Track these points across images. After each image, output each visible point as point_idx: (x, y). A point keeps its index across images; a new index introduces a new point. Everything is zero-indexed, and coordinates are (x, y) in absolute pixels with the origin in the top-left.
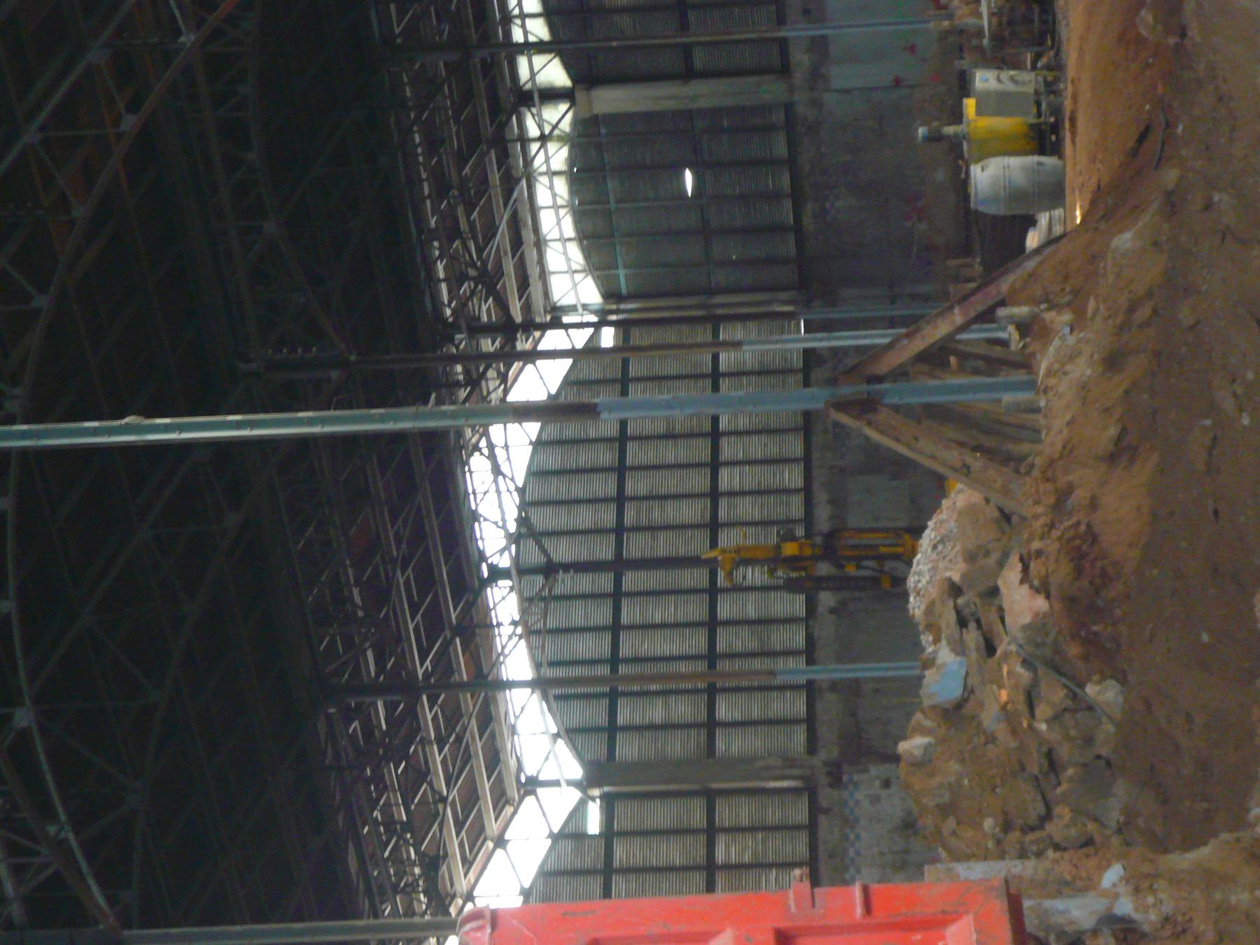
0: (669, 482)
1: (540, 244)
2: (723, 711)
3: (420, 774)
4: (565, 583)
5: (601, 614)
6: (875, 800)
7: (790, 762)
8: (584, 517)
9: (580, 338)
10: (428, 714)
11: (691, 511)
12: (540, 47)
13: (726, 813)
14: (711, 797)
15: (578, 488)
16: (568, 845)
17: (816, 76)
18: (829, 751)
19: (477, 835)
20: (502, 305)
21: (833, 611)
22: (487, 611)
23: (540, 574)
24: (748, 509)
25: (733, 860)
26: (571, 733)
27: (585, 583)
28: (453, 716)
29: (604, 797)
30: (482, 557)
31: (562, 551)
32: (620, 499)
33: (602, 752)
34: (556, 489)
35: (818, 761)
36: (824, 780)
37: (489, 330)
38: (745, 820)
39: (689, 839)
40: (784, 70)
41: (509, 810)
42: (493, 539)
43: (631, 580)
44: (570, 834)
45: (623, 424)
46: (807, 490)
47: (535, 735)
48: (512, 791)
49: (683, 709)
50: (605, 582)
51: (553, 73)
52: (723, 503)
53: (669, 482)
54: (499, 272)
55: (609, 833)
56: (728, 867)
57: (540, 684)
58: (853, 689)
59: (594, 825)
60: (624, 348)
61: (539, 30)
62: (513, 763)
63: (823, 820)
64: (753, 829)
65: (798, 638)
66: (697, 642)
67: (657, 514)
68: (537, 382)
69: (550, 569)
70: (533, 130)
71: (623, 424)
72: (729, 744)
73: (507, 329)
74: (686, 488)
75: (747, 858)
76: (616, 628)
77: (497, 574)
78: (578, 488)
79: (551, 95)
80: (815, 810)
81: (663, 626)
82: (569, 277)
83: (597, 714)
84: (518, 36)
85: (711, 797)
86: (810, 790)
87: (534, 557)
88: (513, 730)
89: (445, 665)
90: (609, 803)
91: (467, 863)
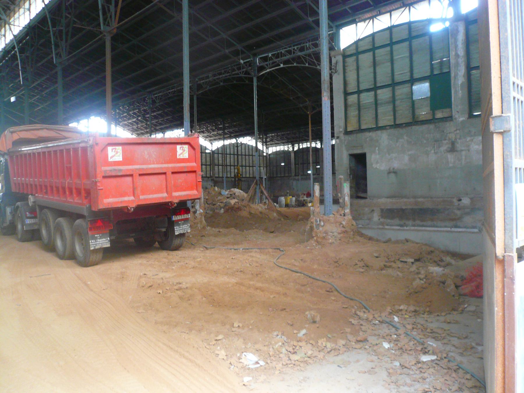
0: (247, 161)
1: (276, 146)
2: (220, 167)
3: (213, 131)
4: (236, 148)
7: (214, 175)
8: (243, 151)
9: (265, 151)
10: (220, 132)
11: (244, 164)
12: (299, 147)
13: (208, 167)
14: (210, 165)
15: (247, 150)
17: (295, 179)
19: (206, 137)
20: (269, 142)
23: (237, 145)
24: (244, 170)
26: (218, 149)
27: (236, 151)
28: (220, 135)
31: (239, 148)
34: (247, 148)
37: (266, 140)
40: (295, 176)
43: (236, 156)
44: (206, 148)
46: (246, 177)
47: (218, 144)
49: (220, 162)
50: (236, 153)
51: (296, 148)
53: (247, 161)
55: (206, 153)
59: (207, 151)
60: (264, 156)
61: (301, 147)
65: (229, 176)
68: (260, 146)
69: (237, 147)
70: (289, 146)
72: (216, 168)
73: (266, 142)
77: (237, 140)
78: (247, 150)
79: (293, 148)
80: (208, 177)
82: (272, 150)
85: (210, 165)
86: (211, 177)
89: (227, 134)
90: (210, 153)
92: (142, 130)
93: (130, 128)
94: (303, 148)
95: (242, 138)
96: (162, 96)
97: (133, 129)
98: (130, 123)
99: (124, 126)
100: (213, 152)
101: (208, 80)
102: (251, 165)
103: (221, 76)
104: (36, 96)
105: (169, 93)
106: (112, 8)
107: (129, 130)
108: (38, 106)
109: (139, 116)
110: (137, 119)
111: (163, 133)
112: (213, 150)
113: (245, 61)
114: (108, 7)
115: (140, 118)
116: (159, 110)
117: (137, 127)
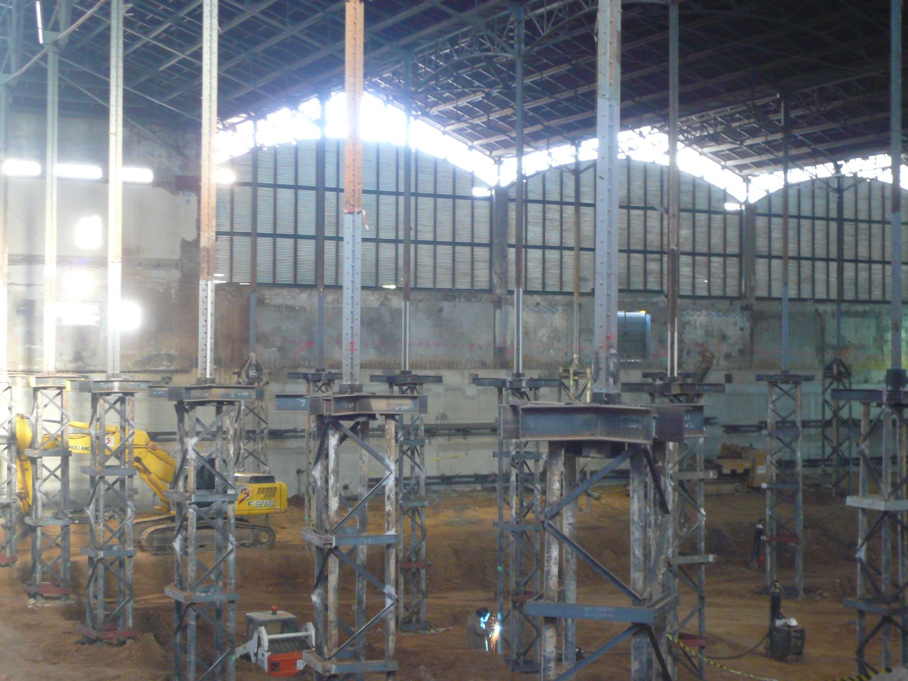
0: (877, 244)
2: (776, 263)
3: (753, 133)
4: (834, 197)
5: (863, 216)
6: (735, 324)
7: (753, 289)
8: (863, 206)
10: (779, 136)
11: (863, 252)
14: (739, 256)
15: (876, 203)
16: (721, 196)
18: (758, 306)
19: (727, 158)
21: (817, 310)
22: (823, 163)
24: (863, 275)
25: (712, 264)
26: (769, 198)
27: (833, 206)
29: (741, 210)
30: (846, 161)
31: (848, 196)
32: (870, 221)
33: (760, 211)
34: (877, 195)
35: (752, 301)
36: (744, 303)
38: (728, 270)
39: (721, 246)
41: (737, 171)
43: (833, 226)
44: (725, 197)
45: (889, 223)
46: (870, 302)
47: (767, 183)
48: (745, 172)
49: (777, 246)
50: (833, 214)
52: (866, 266)
53: (877, 244)
55: (725, 213)
56: (709, 262)
57: (787, 186)
58: (779, 317)
59: (730, 207)
62: (757, 173)
63: (727, 302)
64: (725, 272)
65: (806, 294)
66: (806, 252)
67: (863, 237)
69: (840, 191)
71: (889, 223)
72: (761, 265)
74: (873, 250)
75: (713, 270)
76: (813, 218)
77: (838, 168)
78: (876, 203)
80: (732, 299)
81: (813, 238)
83: (777, 209)
85: (739, 256)
86: (741, 297)
87: (846, 184)
88: (771, 173)
89: (798, 144)
90: (739, 213)
91: (715, 154)
92: (503, 132)
95: (859, 160)
96: (560, 11)
97: (474, 127)
98: (463, 109)
99: (444, 119)
100: (750, 213)
104: (160, 23)
107: (460, 131)
108: (170, 55)
109: (492, 85)
110: (488, 96)
111: (573, 143)
112: (752, 201)
115: (495, 93)
116: (558, 63)
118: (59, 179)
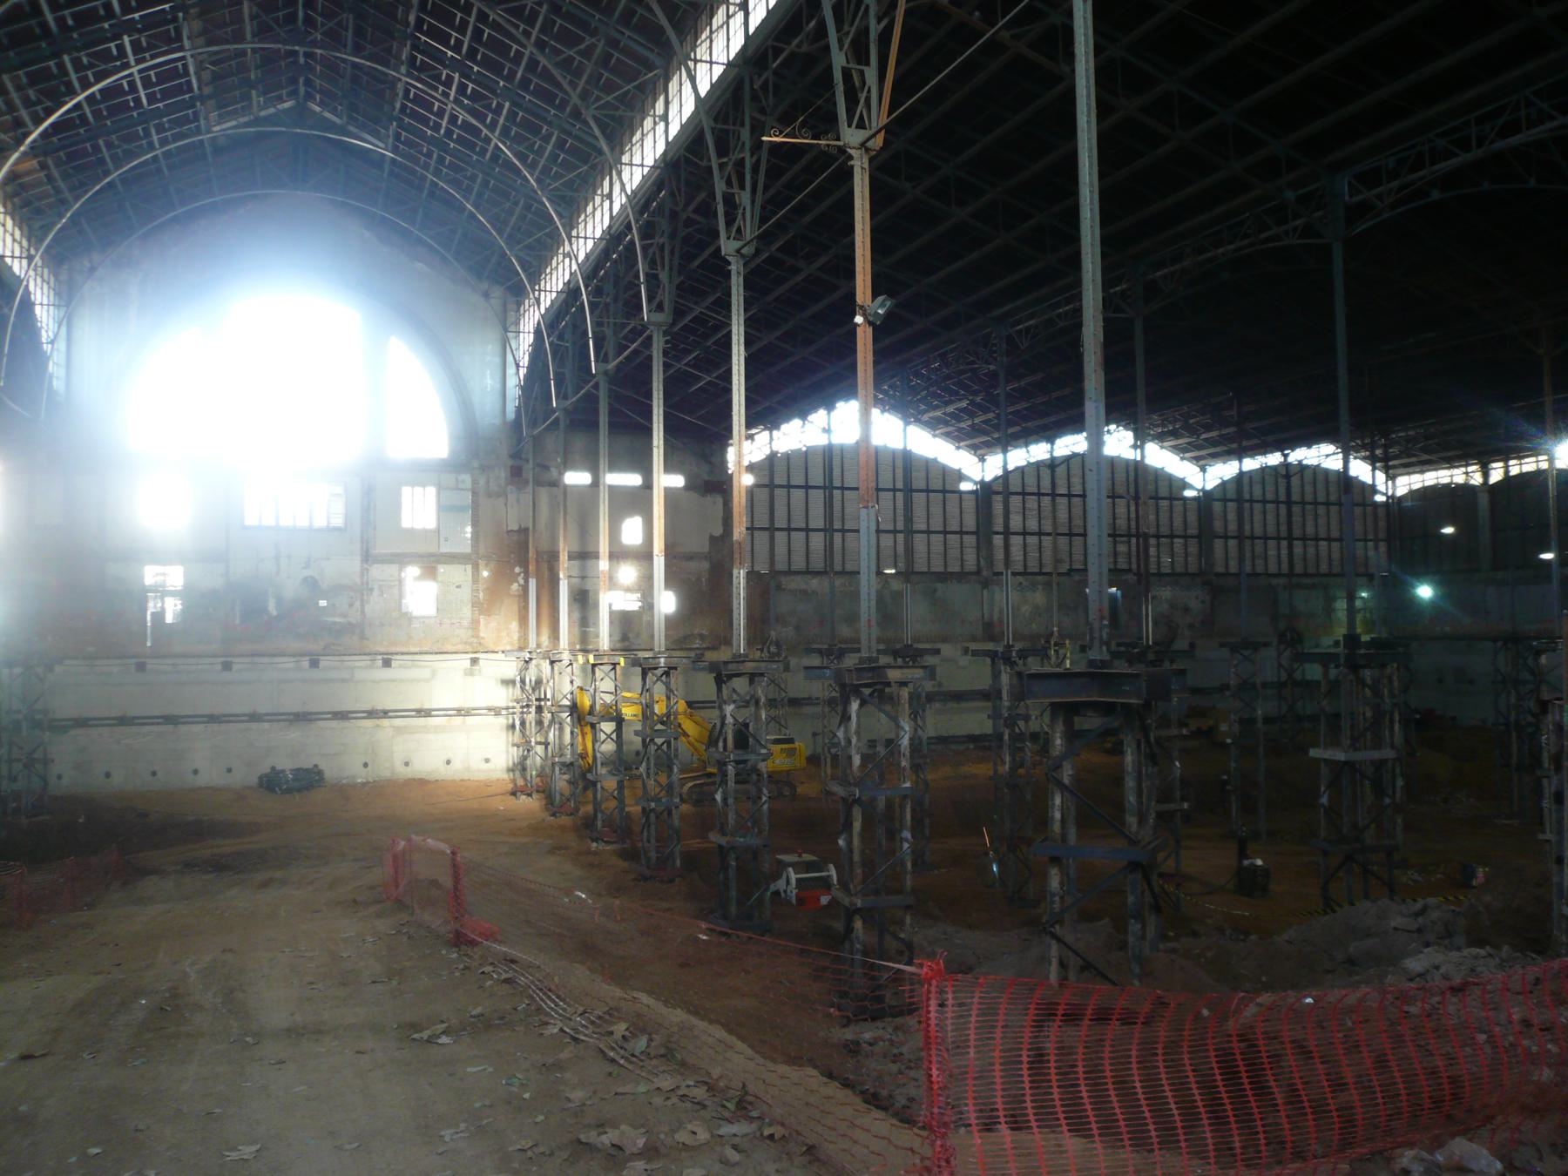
0: (1322, 521)
1: (1422, 472)
3: (1208, 428)
4: (1282, 483)
5: (1309, 498)
8: (1308, 489)
9: (1381, 487)
10: (1231, 430)
12: (1507, 472)
15: (1320, 487)
24: (1311, 551)
26: (1224, 484)
27: (1282, 490)
31: (1295, 481)
32: (1316, 503)
37: (1386, 452)
42: (1300, 455)
43: (1283, 509)
44: (1185, 485)
46: (1318, 575)
47: (1223, 471)
50: (1282, 497)
51: (1496, 475)
53: (1322, 521)
54: (1409, 456)
57: (1241, 474)
61: (1514, 471)
65: (1259, 569)
66: (1258, 531)
68: (1360, 470)
69: (1288, 476)
70: (1470, 469)
72: (1218, 544)
76: (1264, 502)
77: (1286, 456)
79: (1486, 475)
82: (1406, 484)
84: (1512, 462)
85: (1199, 537)
92: (986, 433)
93: (951, 429)
94: (1521, 475)
95: (1304, 449)
97: (960, 430)
98: (950, 415)
99: (932, 425)
100: (1207, 497)
101: (1177, 267)
102: (1335, 534)
103: (1221, 250)
104: (690, 352)
105: (1059, 316)
106: (871, 74)
108: (699, 379)
109: (975, 393)
110: (972, 403)
113: (1301, 192)
114: (862, 73)
115: (978, 399)
117: (972, 426)
118: (666, 490)
